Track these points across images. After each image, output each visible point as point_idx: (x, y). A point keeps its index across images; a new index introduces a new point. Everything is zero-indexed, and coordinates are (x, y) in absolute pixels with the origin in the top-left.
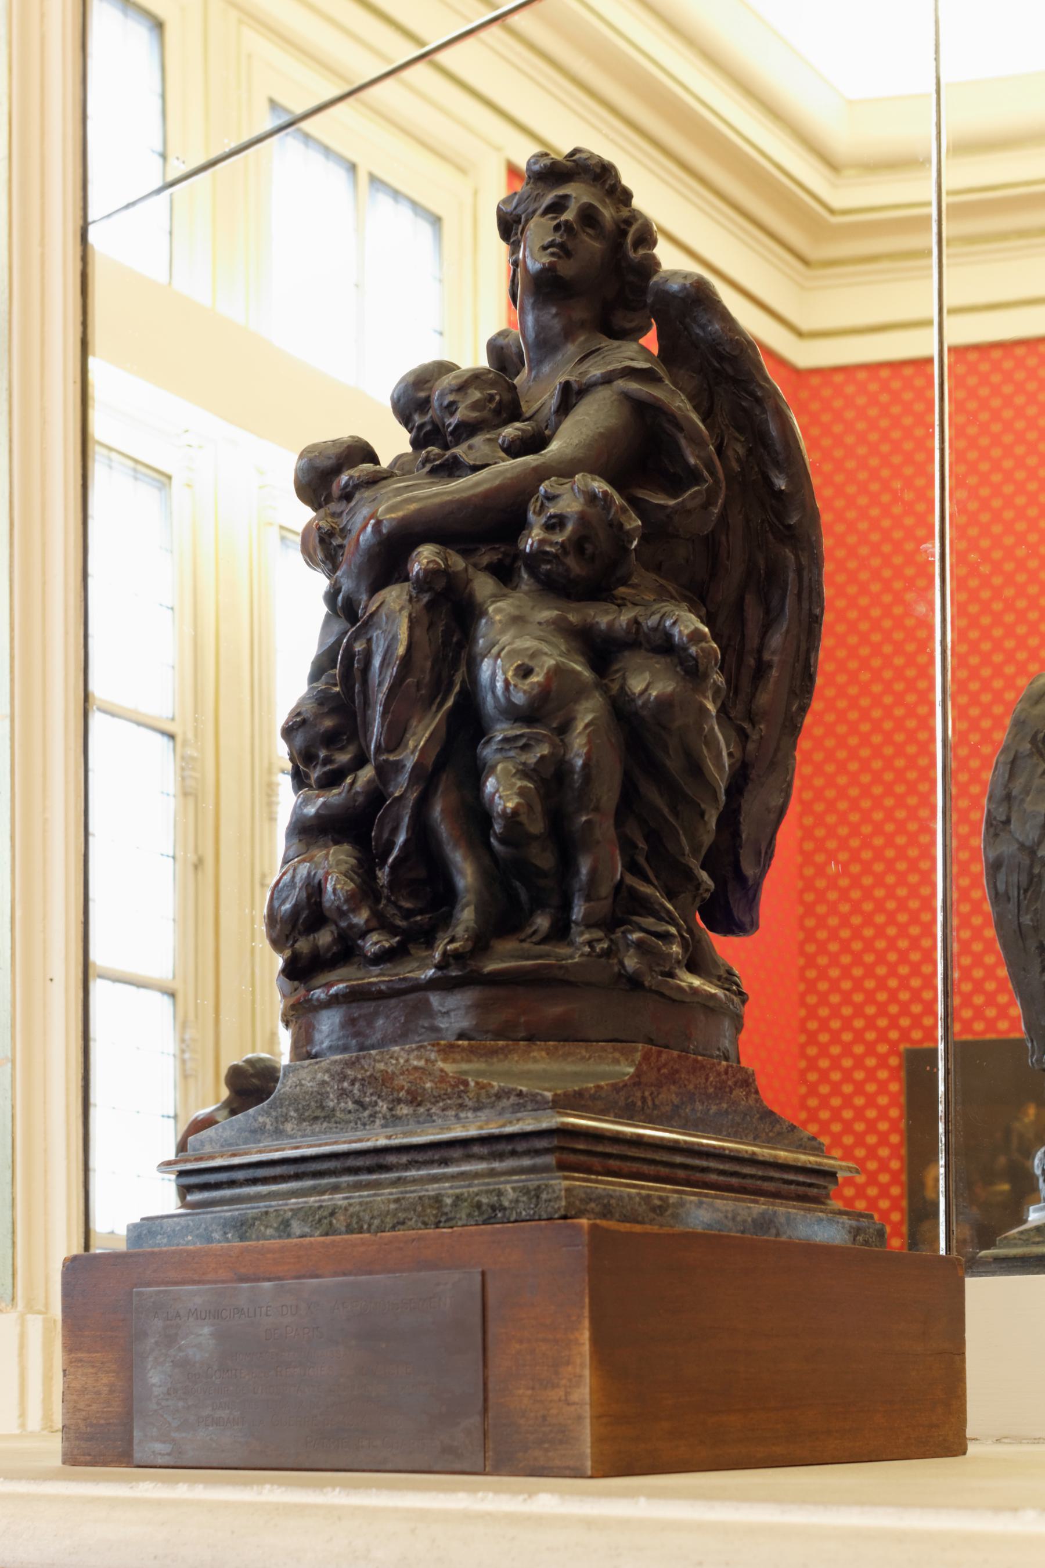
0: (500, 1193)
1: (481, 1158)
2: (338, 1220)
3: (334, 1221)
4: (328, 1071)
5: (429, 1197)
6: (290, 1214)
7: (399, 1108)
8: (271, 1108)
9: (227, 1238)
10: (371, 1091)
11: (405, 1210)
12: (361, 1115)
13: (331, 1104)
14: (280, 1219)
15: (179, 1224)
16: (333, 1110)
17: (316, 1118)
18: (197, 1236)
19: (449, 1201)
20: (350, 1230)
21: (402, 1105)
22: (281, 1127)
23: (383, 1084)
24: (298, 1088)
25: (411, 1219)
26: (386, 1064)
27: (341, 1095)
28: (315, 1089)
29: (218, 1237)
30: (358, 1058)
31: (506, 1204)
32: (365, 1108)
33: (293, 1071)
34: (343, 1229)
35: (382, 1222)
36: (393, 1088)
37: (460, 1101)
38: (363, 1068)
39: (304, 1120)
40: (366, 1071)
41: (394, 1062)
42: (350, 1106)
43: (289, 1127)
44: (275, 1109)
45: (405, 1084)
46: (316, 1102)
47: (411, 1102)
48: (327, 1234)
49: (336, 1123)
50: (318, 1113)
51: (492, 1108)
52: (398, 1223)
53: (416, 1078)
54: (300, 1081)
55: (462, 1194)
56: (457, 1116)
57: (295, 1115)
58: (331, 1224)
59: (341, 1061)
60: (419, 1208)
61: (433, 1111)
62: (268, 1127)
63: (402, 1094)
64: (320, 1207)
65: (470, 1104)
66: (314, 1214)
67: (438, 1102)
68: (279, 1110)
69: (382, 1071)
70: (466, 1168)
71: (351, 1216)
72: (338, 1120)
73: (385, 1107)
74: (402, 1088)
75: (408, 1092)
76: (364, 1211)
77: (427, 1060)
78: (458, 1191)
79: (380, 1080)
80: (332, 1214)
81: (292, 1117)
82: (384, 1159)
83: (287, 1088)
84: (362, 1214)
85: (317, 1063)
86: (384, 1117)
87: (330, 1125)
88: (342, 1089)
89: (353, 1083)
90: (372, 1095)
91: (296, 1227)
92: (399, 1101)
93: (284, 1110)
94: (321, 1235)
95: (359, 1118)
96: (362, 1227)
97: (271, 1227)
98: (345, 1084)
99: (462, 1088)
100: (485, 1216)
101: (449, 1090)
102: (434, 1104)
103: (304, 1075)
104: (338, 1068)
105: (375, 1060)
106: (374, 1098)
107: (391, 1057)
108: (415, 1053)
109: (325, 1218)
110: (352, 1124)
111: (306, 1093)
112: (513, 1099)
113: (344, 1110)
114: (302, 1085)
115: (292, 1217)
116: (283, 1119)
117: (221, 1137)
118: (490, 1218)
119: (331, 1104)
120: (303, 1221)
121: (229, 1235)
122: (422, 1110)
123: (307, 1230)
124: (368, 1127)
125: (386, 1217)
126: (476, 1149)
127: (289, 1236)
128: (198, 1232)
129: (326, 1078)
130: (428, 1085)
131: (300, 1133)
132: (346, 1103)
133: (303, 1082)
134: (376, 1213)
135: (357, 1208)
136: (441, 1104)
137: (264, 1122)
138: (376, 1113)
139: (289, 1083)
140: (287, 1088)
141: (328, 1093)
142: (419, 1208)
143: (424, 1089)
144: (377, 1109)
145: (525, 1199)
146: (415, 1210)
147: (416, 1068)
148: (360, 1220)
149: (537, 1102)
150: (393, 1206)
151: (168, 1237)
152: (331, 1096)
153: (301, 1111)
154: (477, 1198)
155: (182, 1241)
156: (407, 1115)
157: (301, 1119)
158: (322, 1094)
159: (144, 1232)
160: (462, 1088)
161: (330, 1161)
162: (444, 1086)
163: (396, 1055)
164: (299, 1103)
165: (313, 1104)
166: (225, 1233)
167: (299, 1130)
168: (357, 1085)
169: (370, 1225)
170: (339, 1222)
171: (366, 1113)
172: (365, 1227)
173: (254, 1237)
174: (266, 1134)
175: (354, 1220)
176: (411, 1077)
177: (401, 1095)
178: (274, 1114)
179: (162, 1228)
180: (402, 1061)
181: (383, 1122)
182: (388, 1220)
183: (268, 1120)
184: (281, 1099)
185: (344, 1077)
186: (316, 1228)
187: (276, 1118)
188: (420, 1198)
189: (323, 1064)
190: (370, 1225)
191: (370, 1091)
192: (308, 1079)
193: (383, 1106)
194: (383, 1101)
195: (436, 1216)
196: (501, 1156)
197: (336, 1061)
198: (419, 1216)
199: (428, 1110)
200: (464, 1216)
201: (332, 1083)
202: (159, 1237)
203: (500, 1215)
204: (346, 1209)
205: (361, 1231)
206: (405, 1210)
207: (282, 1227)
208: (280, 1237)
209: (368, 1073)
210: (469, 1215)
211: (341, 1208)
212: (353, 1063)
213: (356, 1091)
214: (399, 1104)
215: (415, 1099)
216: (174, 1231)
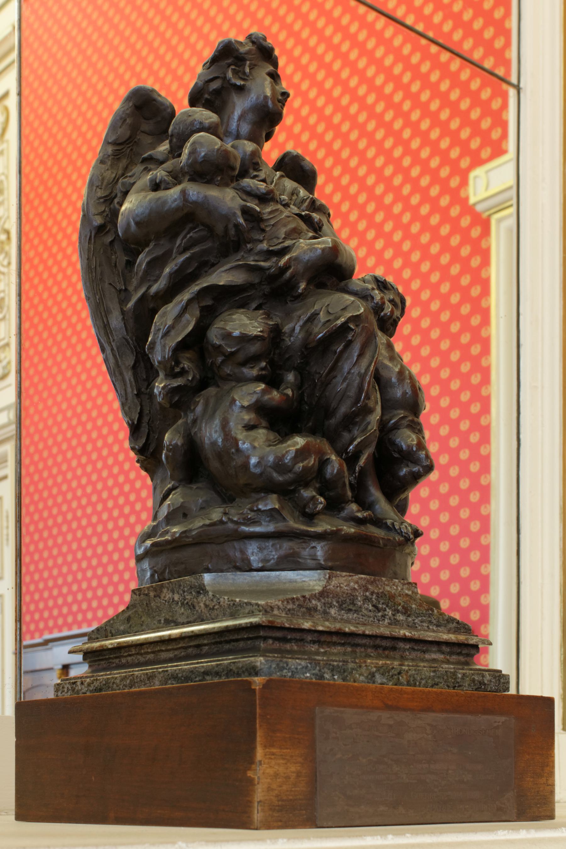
0: (483, 676)
1: (443, 653)
2: (402, 677)
3: (401, 678)
4: (357, 582)
5: (451, 672)
6: (374, 669)
7: (398, 615)
8: (321, 596)
9: (334, 679)
10: (383, 601)
11: (439, 677)
12: (377, 614)
13: (359, 604)
14: (368, 672)
15: (300, 664)
16: (361, 607)
17: (350, 610)
18: (313, 674)
19: (460, 676)
20: (408, 684)
21: (400, 614)
22: (328, 610)
23: (389, 599)
24: (338, 588)
25: (441, 683)
26: (391, 588)
27: (365, 599)
28: (349, 592)
29: (328, 677)
30: (375, 580)
31: (486, 682)
32: (379, 610)
33: (335, 577)
34: (405, 683)
35: (427, 682)
36: (395, 603)
37: (430, 619)
38: (377, 586)
39: (343, 609)
40: (380, 589)
41: (395, 588)
42: (371, 607)
43: (333, 611)
44: (324, 598)
45: (401, 602)
46: (350, 600)
47: (405, 614)
48: (396, 685)
49: (362, 616)
50: (351, 607)
51: (445, 626)
52: (435, 684)
53: (407, 600)
54: (340, 584)
55: (466, 673)
56: (428, 627)
57: (337, 605)
58: (399, 679)
59: (365, 579)
60: (445, 678)
61: (416, 621)
62: (319, 608)
63: (400, 608)
64: (393, 668)
65: (435, 622)
66: (389, 672)
67: (418, 617)
68: (327, 599)
69: (388, 591)
70: (434, 656)
71: (410, 676)
72: (363, 614)
73: (390, 612)
74: (400, 604)
75: (403, 607)
76: (417, 674)
77: (413, 592)
78: (464, 671)
79: (388, 596)
80: (399, 673)
81: (335, 606)
82: (397, 644)
83: (332, 587)
84: (416, 676)
85: (350, 576)
86: (390, 619)
87: (359, 616)
88: (366, 596)
89: (372, 593)
90: (383, 604)
91: (379, 678)
92: (398, 611)
93: (330, 600)
94: (392, 685)
95: (375, 616)
96: (416, 684)
97: (363, 675)
98: (368, 594)
99: (431, 612)
100: (476, 687)
101: (424, 612)
102: (417, 617)
103: (343, 582)
104: (364, 583)
105: (384, 584)
106: (384, 606)
107: (394, 585)
108: (407, 586)
109: (396, 675)
110: (372, 619)
111: (344, 593)
112: (455, 625)
113: (367, 609)
114: (341, 587)
115: (376, 671)
116: (329, 606)
117: (286, 607)
118: (479, 688)
119: (359, 604)
120: (383, 674)
121: (336, 677)
122: (410, 619)
123: (385, 680)
124: (380, 622)
125: (428, 679)
126: (444, 648)
127: (374, 682)
128: (314, 672)
129: (356, 586)
130: (414, 606)
131: (340, 617)
132: (368, 605)
133: (342, 585)
134: (423, 677)
135: (413, 672)
136: (420, 618)
137: (316, 604)
138: (385, 615)
139: (333, 583)
140: (332, 587)
141: (357, 596)
142: (445, 678)
143: (411, 608)
144: (386, 613)
145: (494, 680)
146: (443, 678)
147: (407, 595)
148: (415, 680)
149: (466, 629)
150: (432, 674)
151: (292, 672)
152: (359, 598)
153: (341, 603)
154: (473, 677)
155: (302, 676)
156: (402, 620)
157: (341, 608)
158: (353, 596)
159: (274, 666)
160: (431, 612)
161: (367, 639)
162: (421, 608)
163: (396, 584)
164: (339, 598)
165: (348, 600)
166: (333, 675)
167: (339, 615)
168: (374, 596)
169: (420, 683)
170: (403, 679)
171: (380, 614)
172: (418, 683)
173: (352, 680)
174: (318, 613)
175: (412, 679)
176: (405, 599)
177: (399, 608)
178: (323, 601)
179: (287, 665)
180: (399, 589)
181: (389, 621)
182: (429, 681)
183: (319, 604)
184: (328, 593)
185: (367, 590)
186: (390, 680)
187: (324, 604)
188: (446, 672)
189: (354, 577)
190: (420, 683)
191: (382, 601)
192: (345, 584)
193: (389, 612)
194: (389, 609)
195: (453, 683)
196: (451, 653)
197: (362, 578)
198: (445, 682)
199: (414, 620)
200: (467, 685)
201: (359, 591)
202: (285, 671)
203: (483, 687)
204: (407, 672)
205: (415, 685)
206: (439, 677)
207: (370, 677)
208: (368, 682)
209: (381, 591)
210: (469, 685)
211: (404, 670)
212: (372, 582)
213: (374, 600)
214: (398, 613)
215: (406, 611)
216: (296, 669)
